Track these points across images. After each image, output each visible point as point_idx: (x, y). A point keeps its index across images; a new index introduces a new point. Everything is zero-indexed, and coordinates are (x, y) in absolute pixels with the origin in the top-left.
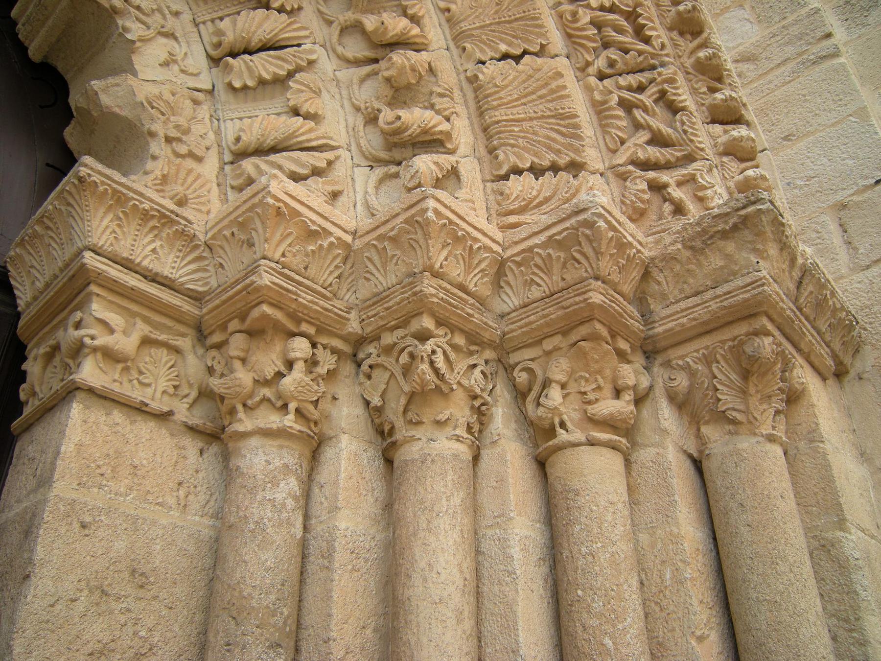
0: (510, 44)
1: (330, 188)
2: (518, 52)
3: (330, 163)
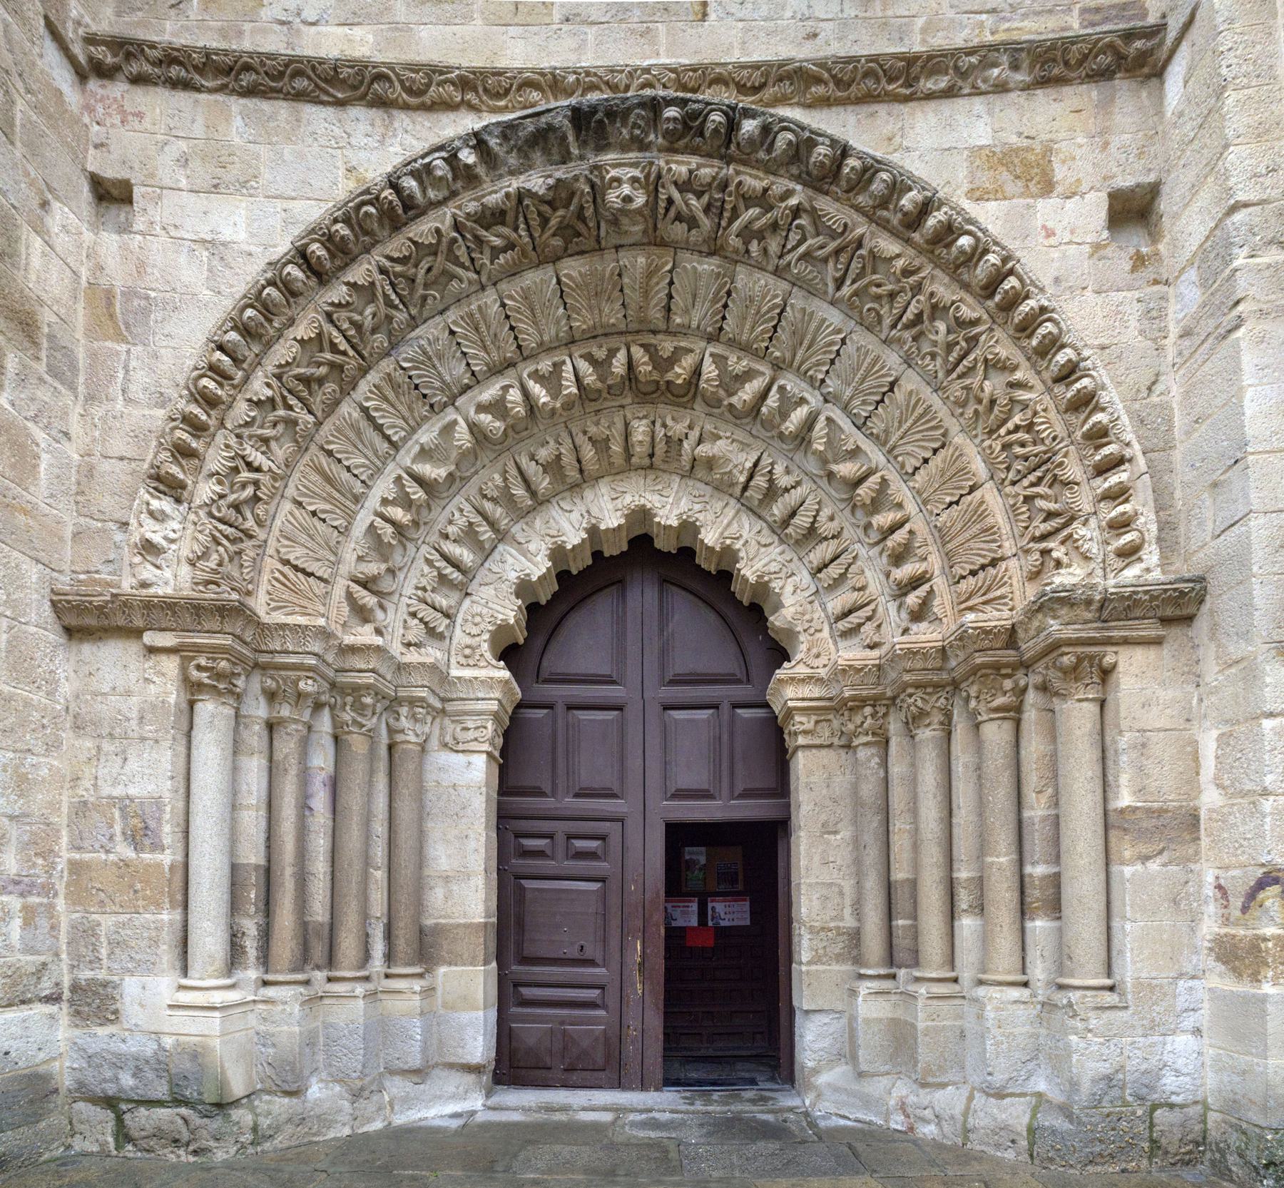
0: (952, 495)
2: (955, 499)
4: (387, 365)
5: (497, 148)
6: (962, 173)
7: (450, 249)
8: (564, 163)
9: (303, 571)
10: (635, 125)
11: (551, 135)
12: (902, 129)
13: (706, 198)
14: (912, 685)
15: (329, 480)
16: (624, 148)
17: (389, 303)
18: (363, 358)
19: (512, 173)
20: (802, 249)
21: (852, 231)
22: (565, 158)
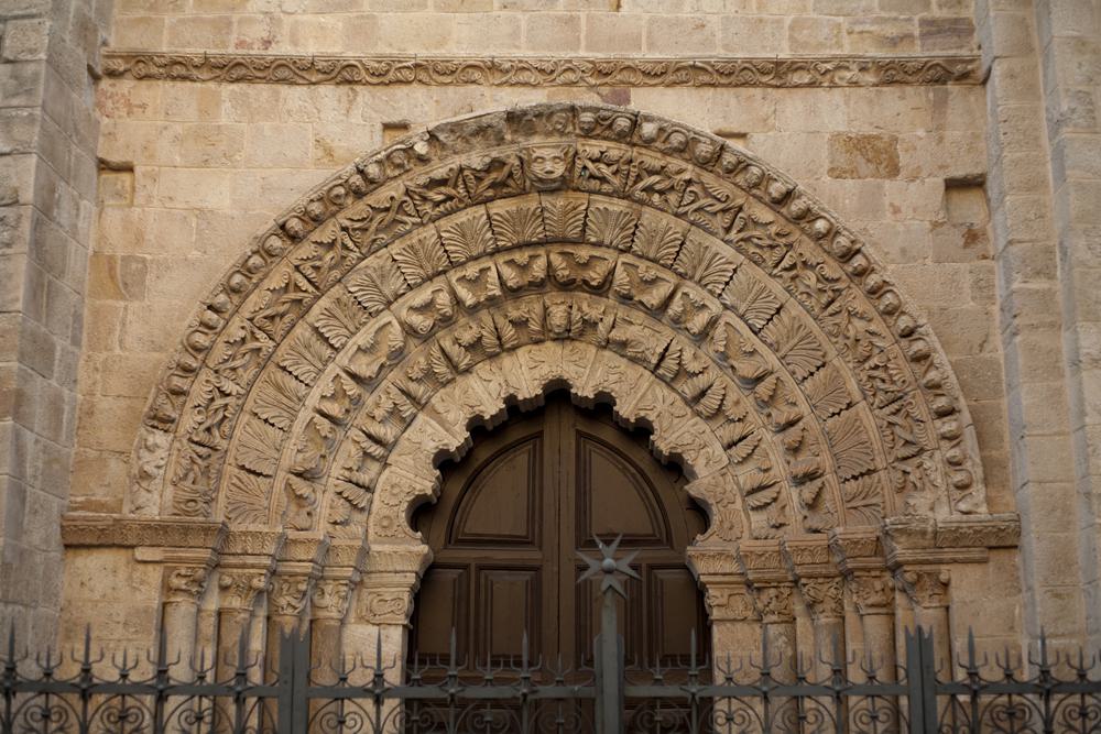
1: (780, 506)
2: (837, 411)
3: (779, 493)
4: (337, 291)
5: (445, 140)
6: (825, 153)
7: (400, 205)
8: (498, 145)
9: (254, 473)
10: (557, 122)
11: (490, 131)
12: (775, 111)
13: (614, 168)
14: (803, 577)
15: (279, 389)
16: (549, 134)
17: (345, 247)
18: (317, 288)
19: (455, 153)
20: (695, 206)
21: (733, 200)
22: (500, 140)
